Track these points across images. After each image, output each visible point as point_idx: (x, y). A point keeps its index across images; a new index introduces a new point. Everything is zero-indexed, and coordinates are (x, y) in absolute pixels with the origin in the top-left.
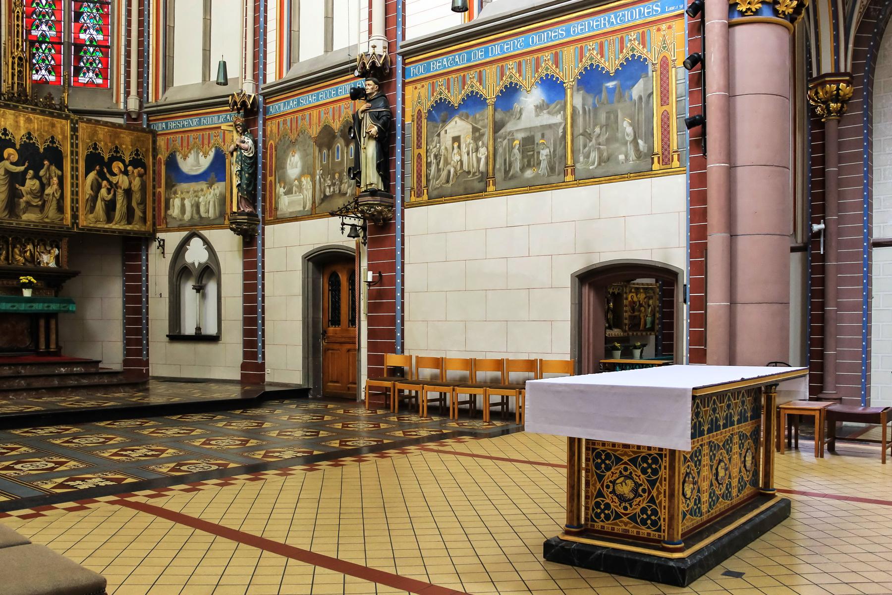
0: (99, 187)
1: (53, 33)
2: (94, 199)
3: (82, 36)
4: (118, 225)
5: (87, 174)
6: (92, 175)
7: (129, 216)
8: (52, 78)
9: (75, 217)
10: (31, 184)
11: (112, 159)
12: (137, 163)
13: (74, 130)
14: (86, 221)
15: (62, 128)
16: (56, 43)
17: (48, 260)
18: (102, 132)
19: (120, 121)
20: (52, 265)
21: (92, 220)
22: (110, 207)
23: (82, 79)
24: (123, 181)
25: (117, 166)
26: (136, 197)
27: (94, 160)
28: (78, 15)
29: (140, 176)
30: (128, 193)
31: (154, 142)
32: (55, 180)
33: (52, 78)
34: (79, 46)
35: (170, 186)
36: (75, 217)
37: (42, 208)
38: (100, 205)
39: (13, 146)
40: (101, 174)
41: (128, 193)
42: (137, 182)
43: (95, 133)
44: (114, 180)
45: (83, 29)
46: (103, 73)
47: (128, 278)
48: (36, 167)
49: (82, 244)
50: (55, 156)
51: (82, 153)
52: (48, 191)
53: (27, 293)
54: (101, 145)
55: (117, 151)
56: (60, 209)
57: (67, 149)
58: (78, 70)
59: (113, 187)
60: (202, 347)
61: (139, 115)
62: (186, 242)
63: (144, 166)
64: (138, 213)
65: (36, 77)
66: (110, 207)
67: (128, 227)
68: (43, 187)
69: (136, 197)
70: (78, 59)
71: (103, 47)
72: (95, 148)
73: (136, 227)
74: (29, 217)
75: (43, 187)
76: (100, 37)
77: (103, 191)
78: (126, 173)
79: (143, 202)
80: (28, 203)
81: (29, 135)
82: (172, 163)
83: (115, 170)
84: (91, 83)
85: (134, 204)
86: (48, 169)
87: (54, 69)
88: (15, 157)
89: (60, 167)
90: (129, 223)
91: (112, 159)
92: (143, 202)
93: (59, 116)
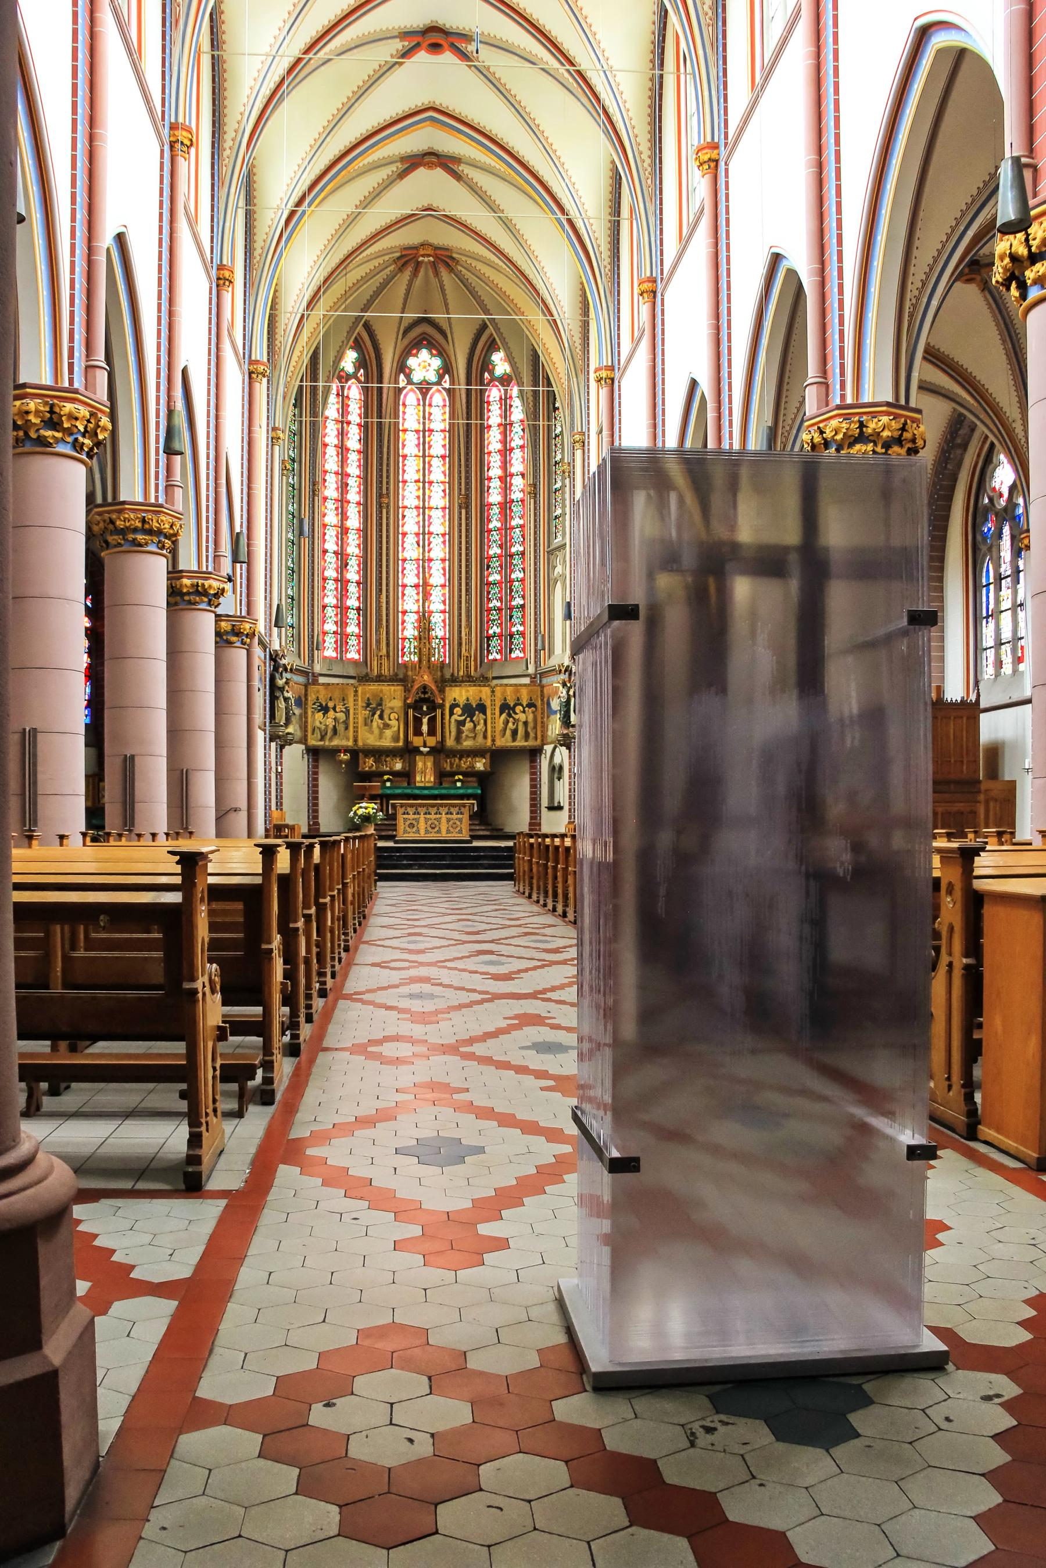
0: (508, 722)
1: (498, 630)
2: (505, 729)
3: (514, 629)
4: (520, 743)
5: (501, 714)
6: (504, 715)
7: (527, 736)
8: (498, 657)
9: (493, 741)
10: (469, 725)
11: (515, 705)
12: (531, 705)
13: (493, 692)
14: (500, 743)
15: (486, 691)
16: (500, 636)
17: (480, 765)
18: (509, 690)
19: (526, 681)
20: (482, 768)
21: (504, 742)
22: (515, 733)
23: (513, 656)
24: (522, 717)
25: (519, 709)
26: (531, 725)
27: (505, 708)
28: (511, 617)
29: (533, 712)
30: (526, 723)
31: (542, 691)
32: (482, 722)
33: (498, 657)
34: (511, 635)
35: (548, 717)
36: (493, 741)
37: (474, 738)
38: (508, 733)
39: (457, 705)
40: (509, 715)
41: (526, 723)
42: (531, 717)
43: (504, 693)
44: (516, 717)
45: (512, 625)
46: (523, 650)
47: (532, 774)
48: (471, 716)
49: (500, 757)
50: (482, 708)
51: (498, 704)
52: (478, 728)
53: (459, 784)
54: (508, 698)
55: (518, 699)
56: (485, 737)
57: (488, 704)
58: (511, 650)
59: (516, 721)
60: (558, 813)
61: (536, 675)
62: (555, 748)
63: (535, 706)
64: (532, 735)
65: (491, 657)
66: (515, 733)
67: (526, 744)
68: (475, 726)
69: (531, 725)
70: (511, 643)
71: (523, 634)
72: (505, 699)
73: (531, 743)
74: (467, 744)
75: (475, 726)
76: (521, 629)
77: (510, 725)
78: (524, 712)
79: (535, 727)
80: (467, 736)
81: (468, 699)
82: (549, 704)
83: (517, 711)
84: (517, 658)
85: (529, 730)
86: (479, 717)
87: (500, 651)
88: (460, 712)
89: (485, 714)
90: (526, 741)
91: (515, 705)
92: (535, 727)
93: (484, 686)
